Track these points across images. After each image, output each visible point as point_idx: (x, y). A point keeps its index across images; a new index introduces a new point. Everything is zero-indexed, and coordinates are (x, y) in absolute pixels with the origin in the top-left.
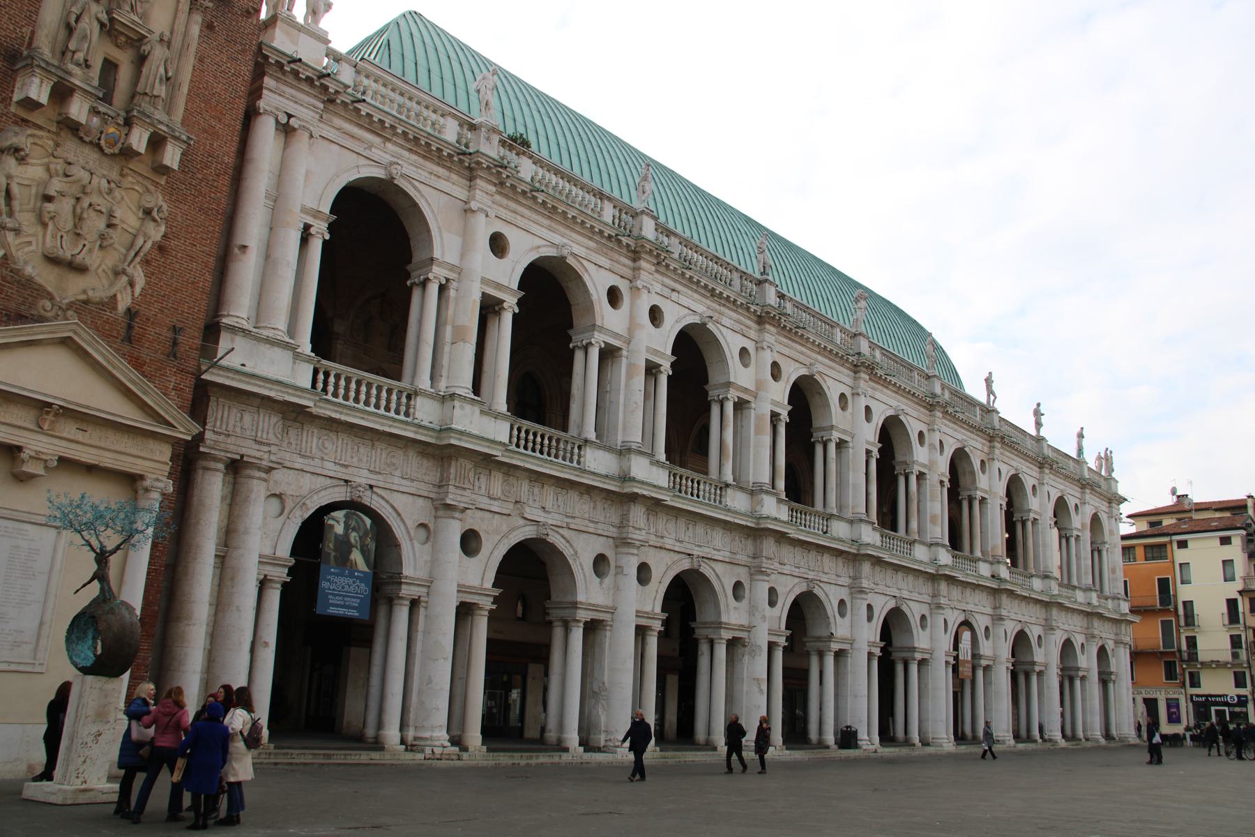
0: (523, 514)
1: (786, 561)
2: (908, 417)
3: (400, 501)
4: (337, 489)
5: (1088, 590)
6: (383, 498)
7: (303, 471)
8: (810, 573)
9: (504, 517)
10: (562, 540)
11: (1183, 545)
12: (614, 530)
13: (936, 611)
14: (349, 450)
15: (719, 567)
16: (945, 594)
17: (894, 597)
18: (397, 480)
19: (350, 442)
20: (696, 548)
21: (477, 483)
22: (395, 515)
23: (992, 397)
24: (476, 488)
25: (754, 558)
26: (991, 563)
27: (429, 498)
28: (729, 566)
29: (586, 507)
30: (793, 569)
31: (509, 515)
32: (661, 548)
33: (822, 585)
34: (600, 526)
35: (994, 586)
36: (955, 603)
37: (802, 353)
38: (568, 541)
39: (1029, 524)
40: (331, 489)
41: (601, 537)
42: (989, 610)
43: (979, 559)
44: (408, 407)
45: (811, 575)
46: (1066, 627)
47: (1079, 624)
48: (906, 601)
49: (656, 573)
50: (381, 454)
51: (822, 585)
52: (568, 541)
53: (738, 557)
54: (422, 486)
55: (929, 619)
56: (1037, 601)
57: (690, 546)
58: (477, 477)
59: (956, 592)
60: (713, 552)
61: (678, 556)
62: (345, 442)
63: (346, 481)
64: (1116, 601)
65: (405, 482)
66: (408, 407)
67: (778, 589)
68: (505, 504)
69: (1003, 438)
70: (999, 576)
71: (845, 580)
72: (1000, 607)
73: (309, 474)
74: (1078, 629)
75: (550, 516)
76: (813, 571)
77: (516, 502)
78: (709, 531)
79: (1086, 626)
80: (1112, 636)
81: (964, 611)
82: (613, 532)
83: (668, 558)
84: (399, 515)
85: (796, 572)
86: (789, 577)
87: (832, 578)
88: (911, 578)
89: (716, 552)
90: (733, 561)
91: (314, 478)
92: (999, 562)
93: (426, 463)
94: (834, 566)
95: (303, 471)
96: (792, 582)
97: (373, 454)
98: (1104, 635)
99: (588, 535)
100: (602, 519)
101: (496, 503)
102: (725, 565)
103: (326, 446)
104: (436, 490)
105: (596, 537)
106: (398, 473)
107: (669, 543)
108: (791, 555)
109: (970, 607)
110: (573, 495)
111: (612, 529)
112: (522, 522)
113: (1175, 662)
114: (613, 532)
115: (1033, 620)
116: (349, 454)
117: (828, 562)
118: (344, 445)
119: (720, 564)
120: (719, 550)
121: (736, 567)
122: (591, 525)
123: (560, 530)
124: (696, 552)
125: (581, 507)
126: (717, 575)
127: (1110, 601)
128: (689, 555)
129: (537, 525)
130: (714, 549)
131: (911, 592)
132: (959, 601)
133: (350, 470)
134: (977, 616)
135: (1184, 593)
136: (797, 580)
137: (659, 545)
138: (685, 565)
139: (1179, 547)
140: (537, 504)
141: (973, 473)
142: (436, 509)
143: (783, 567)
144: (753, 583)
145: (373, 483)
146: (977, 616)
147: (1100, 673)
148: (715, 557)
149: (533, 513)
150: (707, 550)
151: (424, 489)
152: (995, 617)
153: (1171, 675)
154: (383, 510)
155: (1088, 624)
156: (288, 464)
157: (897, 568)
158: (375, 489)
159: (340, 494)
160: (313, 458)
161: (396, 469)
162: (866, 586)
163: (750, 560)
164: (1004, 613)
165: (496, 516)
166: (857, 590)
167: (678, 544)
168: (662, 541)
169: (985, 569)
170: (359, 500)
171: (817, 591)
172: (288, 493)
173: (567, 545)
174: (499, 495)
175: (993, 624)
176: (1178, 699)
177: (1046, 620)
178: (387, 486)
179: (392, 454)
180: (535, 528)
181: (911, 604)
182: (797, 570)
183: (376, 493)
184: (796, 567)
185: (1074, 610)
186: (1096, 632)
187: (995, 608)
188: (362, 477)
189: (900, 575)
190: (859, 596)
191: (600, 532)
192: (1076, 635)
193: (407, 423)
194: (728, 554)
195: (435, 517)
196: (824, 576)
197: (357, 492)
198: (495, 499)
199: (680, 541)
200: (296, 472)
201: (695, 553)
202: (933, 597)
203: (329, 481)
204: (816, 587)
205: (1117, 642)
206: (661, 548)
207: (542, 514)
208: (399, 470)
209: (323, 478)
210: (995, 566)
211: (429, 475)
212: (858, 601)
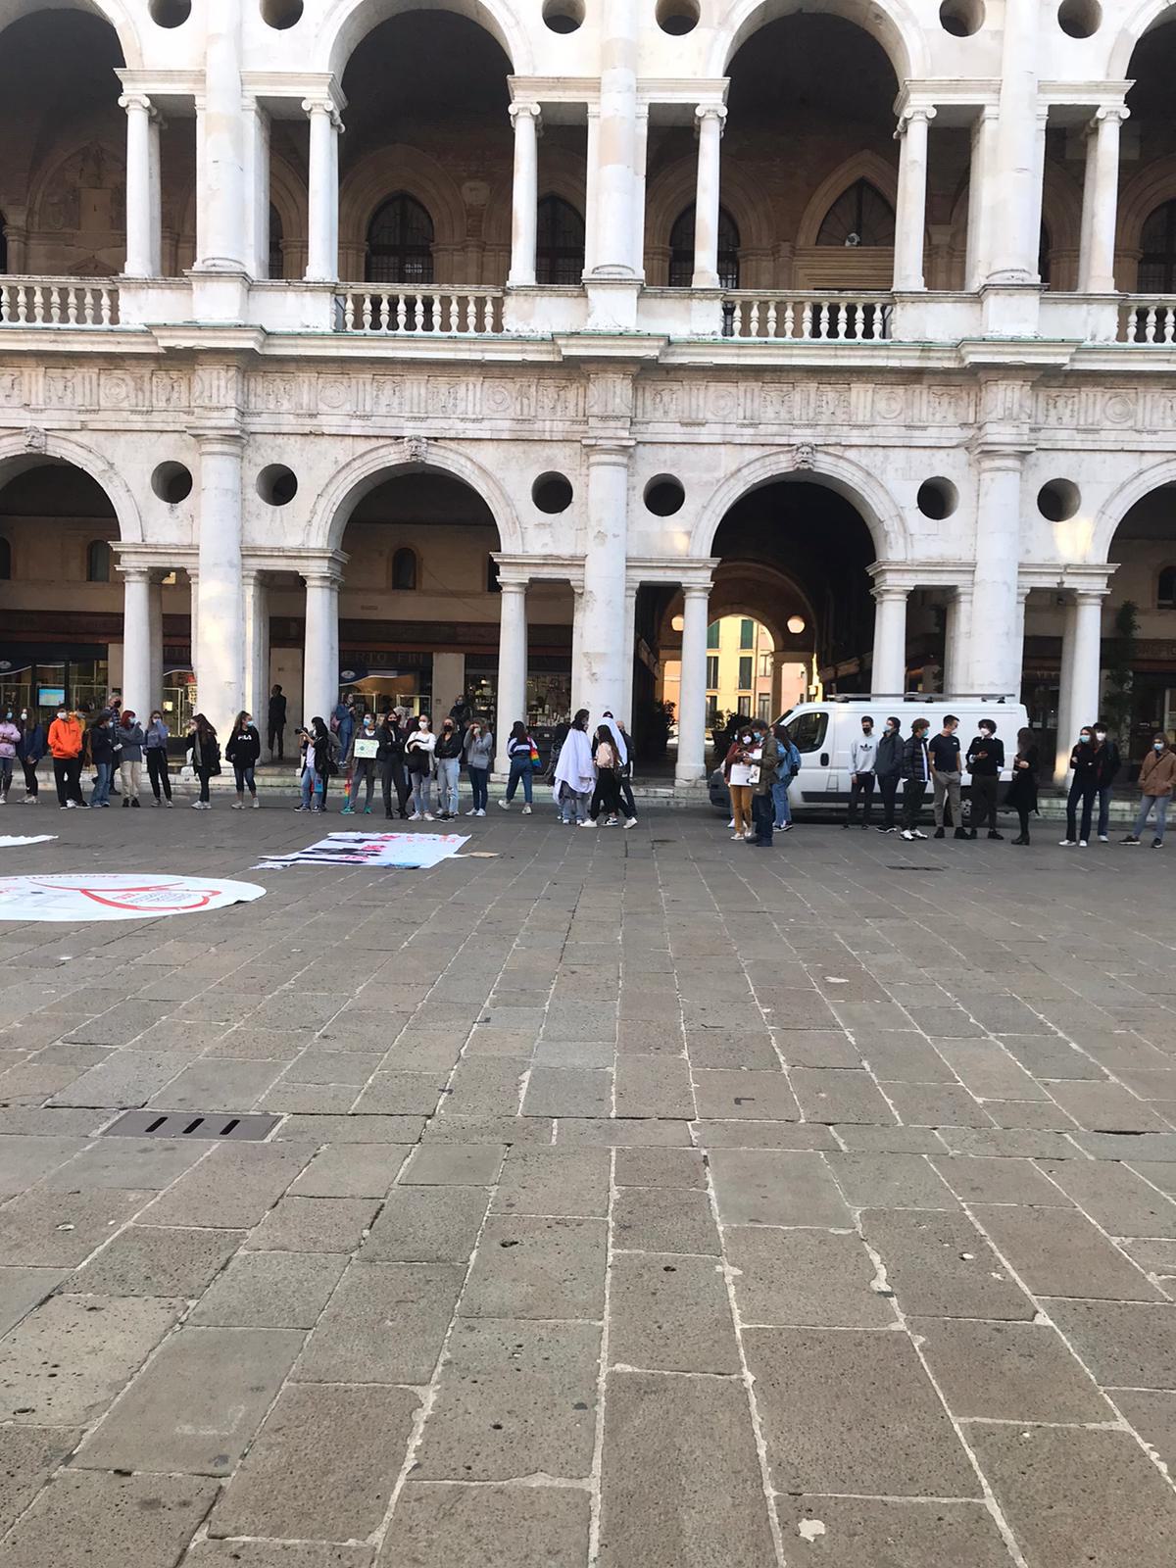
53: (538, 426)
60: (460, 425)
75: (43, 416)
89: (469, 425)
128: (398, 438)
191: (159, 427)
207: (28, 415)
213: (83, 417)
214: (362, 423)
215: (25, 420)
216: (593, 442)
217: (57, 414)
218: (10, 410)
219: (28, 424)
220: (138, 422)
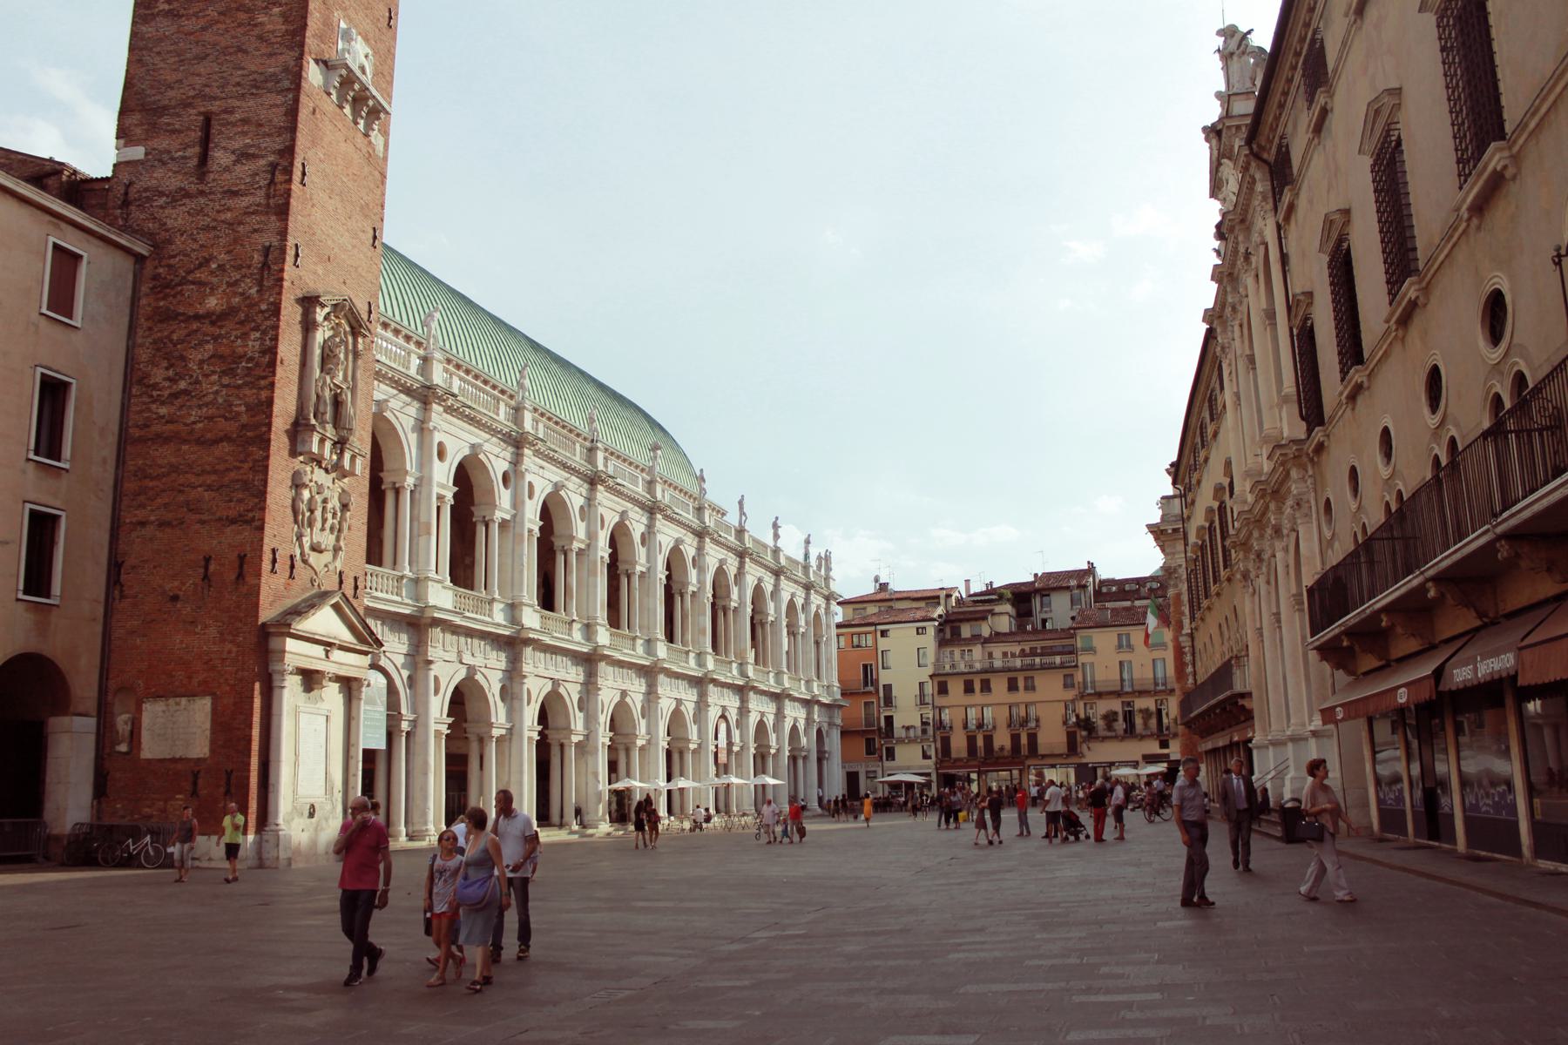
11: (884, 634)
23: (744, 518)
37: (618, 504)
38: (486, 678)
52: (486, 678)
69: (752, 554)
80: (827, 719)
113: (874, 739)
135: (884, 678)
139: (882, 636)
141: (728, 586)
147: (818, 752)
153: (870, 750)
176: (875, 772)
205: (831, 724)
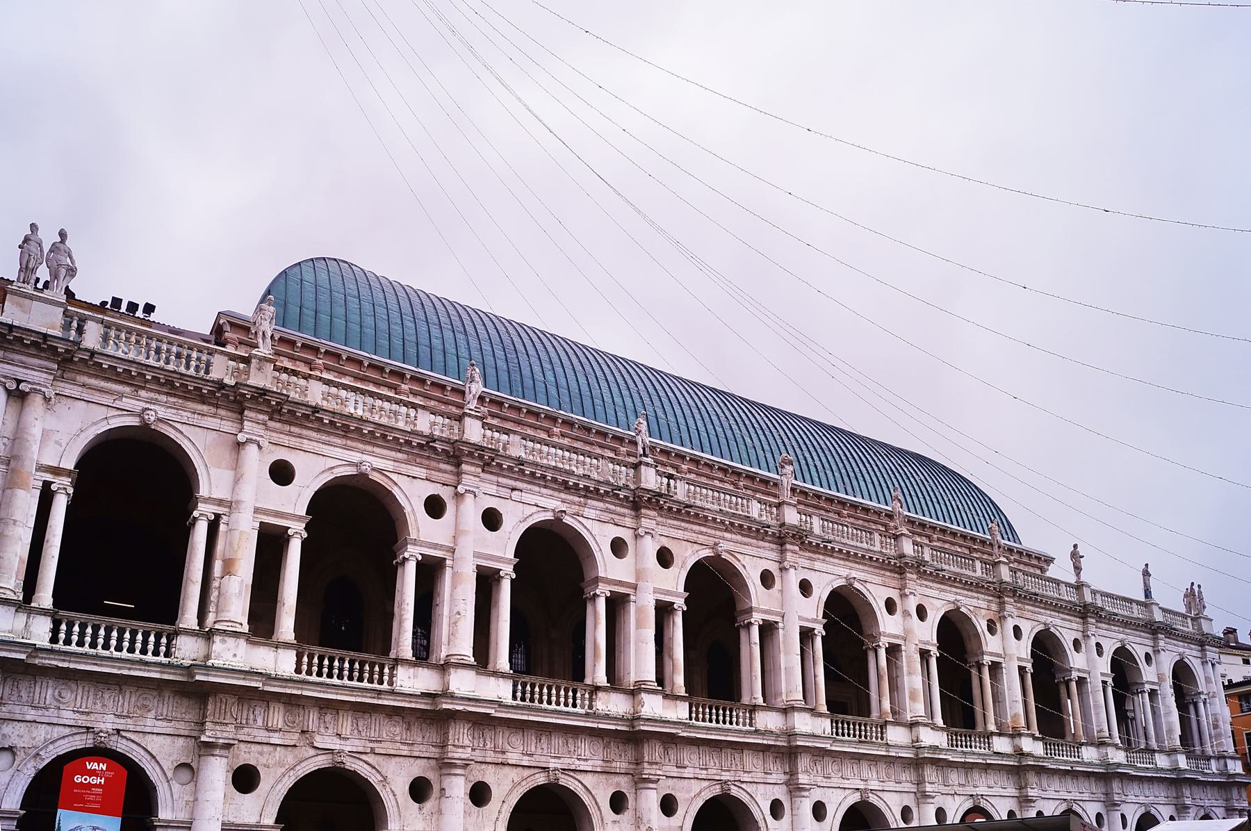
0: (313, 743)
1: (686, 763)
2: (868, 585)
3: (154, 744)
4: (77, 737)
5: (1172, 752)
6: (133, 741)
7: (35, 721)
8: (723, 773)
9: (290, 749)
10: (366, 766)
12: (437, 750)
13: (923, 800)
14: (91, 697)
15: (588, 780)
16: (933, 779)
17: (858, 789)
18: (149, 722)
19: (92, 690)
20: (553, 760)
21: (251, 717)
22: (149, 758)
24: (251, 722)
25: (637, 764)
26: (1012, 736)
27: (191, 737)
28: (603, 777)
29: (398, 730)
30: (698, 771)
31: (295, 746)
32: (502, 764)
33: (744, 786)
34: (416, 748)
35: (1012, 763)
36: (956, 788)
38: (374, 768)
39: (1073, 685)
40: (70, 737)
41: (419, 761)
42: (1012, 791)
43: (992, 734)
44: (168, 646)
45: (726, 776)
46: (1142, 799)
47: (1162, 795)
48: (879, 793)
49: (497, 793)
50: (130, 697)
51: (744, 786)
52: (374, 768)
53: (614, 764)
54: (182, 725)
55: (915, 810)
56: (1088, 775)
57: (543, 759)
58: (252, 710)
59: (954, 777)
60: (577, 762)
61: (527, 772)
62: (86, 689)
63: (88, 728)
64: (1222, 761)
65: (159, 723)
66: (168, 646)
67: (679, 796)
68: (288, 736)
70: (1021, 750)
71: (778, 776)
72: (1026, 787)
73: (44, 726)
74: (1162, 800)
75: (348, 742)
76: (729, 771)
77: (303, 732)
78: (570, 741)
79: (1175, 795)
80: (1221, 803)
81: (972, 795)
82: (434, 752)
83: (514, 774)
84: (154, 757)
85: (703, 774)
86: (692, 780)
87: (759, 776)
88: (882, 766)
89: (582, 762)
90: (608, 770)
91: (48, 727)
92: (1020, 735)
93: (185, 702)
94: (761, 763)
95: (35, 721)
96: (696, 786)
97: (120, 698)
98: (1207, 803)
99: (401, 759)
100: (420, 739)
101: (276, 735)
102: (597, 775)
103: (62, 695)
104: (197, 728)
105: (412, 760)
106: (152, 714)
107: (513, 757)
108: (695, 757)
109: (982, 790)
110: (380, 718)
111: (433, 749)
112: (312, 752)
114: (434, 752)
115: (1086, 796)
116: (90, 701)
117: (750, 760)
118: (86, 693)
119: (590, 775)
120: (586, 760)
121: (612, 776)
122: (405, 747)
123: (364, 757)
124: (553, 764)
125: (391, 731)
126: (585, 787)
127: (1213, 761)
129: (333, 753)
130: (579, 759)
131: (883, 782)
132: (960, 785)
133: (93, 717)
134: (992, 800)
136: (706, 784)
137: (500, 761)
138: (541, 779)
140: (330, 731)
142: (199, 746)
143: (682, 770)
144: (638, 792)
145: (120, 727)
146: (992, 800)
148: (582, 768)
149: (325, 740)
150: (569, 761)
151: (183, 728)
152: (1021, 799)
154: (134, 753)
155: (1177, 793)
156: (19, 717)
157: (858, 758)
158: (121, 732)
159: (79, 742)
160: (47, 709)
161: (149, 711)
162: (806, 782)
163: (631, 766)
164: (1031, 793)
165: (278, 748)
166: (795, 789)
167: (527, 758)
168: (504, 757)
169: (1002, 745)
170: (102, 745)
171: (734, 791)
172: (18, 746)
173: (374, 771)
174: (279, 727)
175: (1021, 807)
177: (1107, 794)
178: (138, 729)
179: (144, 696)
180: (330, 756)
181: (885, 796)
182: (705, 772)
183: (125, 737)
184: (702, 769)
185: (1151, 780)
186: (1188, 802)
187: (1021, 788)
188: (107, 723)
189: (864, 764)
190: (797, 793)
191: (416, 754)
192: (1160, 808)
193: (169, 665)
194: (600, 763)
195: (200, 756)
196: (746, 775)
197: (99, 739)
198: (275, 731)
199: (531, 755)
200: (29, 724)
201: (551, 766)
202: (918, 784)
203: (67, 731)
204: (732, 787)
206: (502, 764)
207: (338, 741)
208: (153, 712)
209: (61, 729)
210: (1017, 740)
211: (189, 713)
212: (796, 799)
213: (372, 745)
214: (530, 758)
215: (335, 744)
216: (647, 776)
217: (357, 742)
218: (328, 737)
219: (337, 747)
220: (405, 750)
